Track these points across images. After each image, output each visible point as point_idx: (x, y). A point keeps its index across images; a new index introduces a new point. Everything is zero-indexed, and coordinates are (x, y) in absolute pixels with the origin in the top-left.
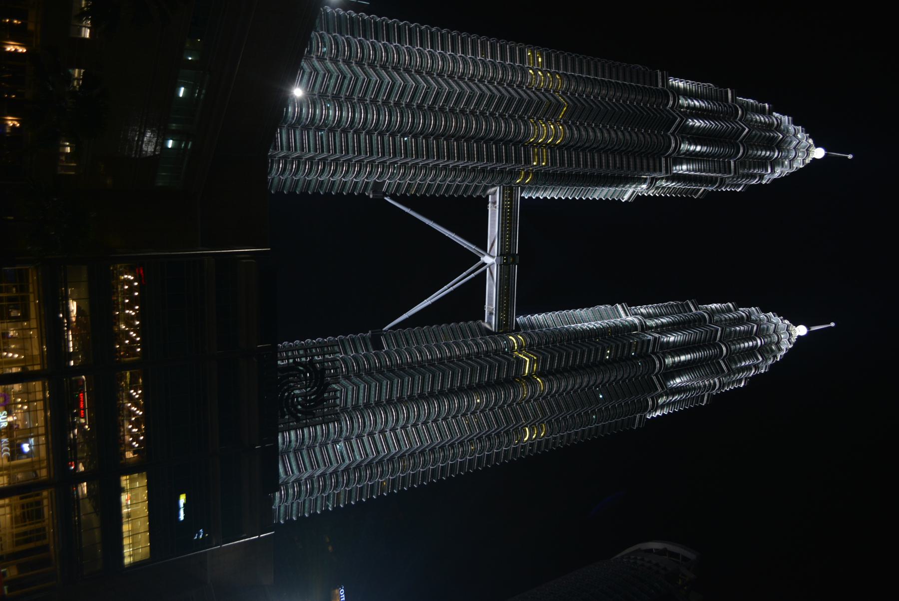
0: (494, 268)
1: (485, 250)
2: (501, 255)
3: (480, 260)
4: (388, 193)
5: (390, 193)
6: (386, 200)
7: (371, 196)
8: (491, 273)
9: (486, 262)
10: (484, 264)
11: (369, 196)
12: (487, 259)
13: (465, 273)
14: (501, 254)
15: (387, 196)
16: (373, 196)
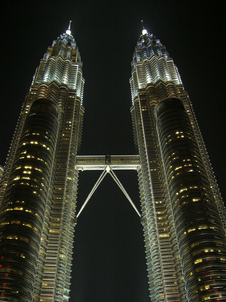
0: (112, 166)
1: (102, 171)
2: (106, 163)
3: (109, 173)
4: (75, 216)
5: (75, 215)
6: (78, 217)
7: (76, 224)
8: (115, 167)
9: (109, 170)
10: (110, 171)
11: (76, 225)
12: (108, 170)
13: (115, 179)
14: (106, 163)
15: (76, 217)
16: (76, 223)
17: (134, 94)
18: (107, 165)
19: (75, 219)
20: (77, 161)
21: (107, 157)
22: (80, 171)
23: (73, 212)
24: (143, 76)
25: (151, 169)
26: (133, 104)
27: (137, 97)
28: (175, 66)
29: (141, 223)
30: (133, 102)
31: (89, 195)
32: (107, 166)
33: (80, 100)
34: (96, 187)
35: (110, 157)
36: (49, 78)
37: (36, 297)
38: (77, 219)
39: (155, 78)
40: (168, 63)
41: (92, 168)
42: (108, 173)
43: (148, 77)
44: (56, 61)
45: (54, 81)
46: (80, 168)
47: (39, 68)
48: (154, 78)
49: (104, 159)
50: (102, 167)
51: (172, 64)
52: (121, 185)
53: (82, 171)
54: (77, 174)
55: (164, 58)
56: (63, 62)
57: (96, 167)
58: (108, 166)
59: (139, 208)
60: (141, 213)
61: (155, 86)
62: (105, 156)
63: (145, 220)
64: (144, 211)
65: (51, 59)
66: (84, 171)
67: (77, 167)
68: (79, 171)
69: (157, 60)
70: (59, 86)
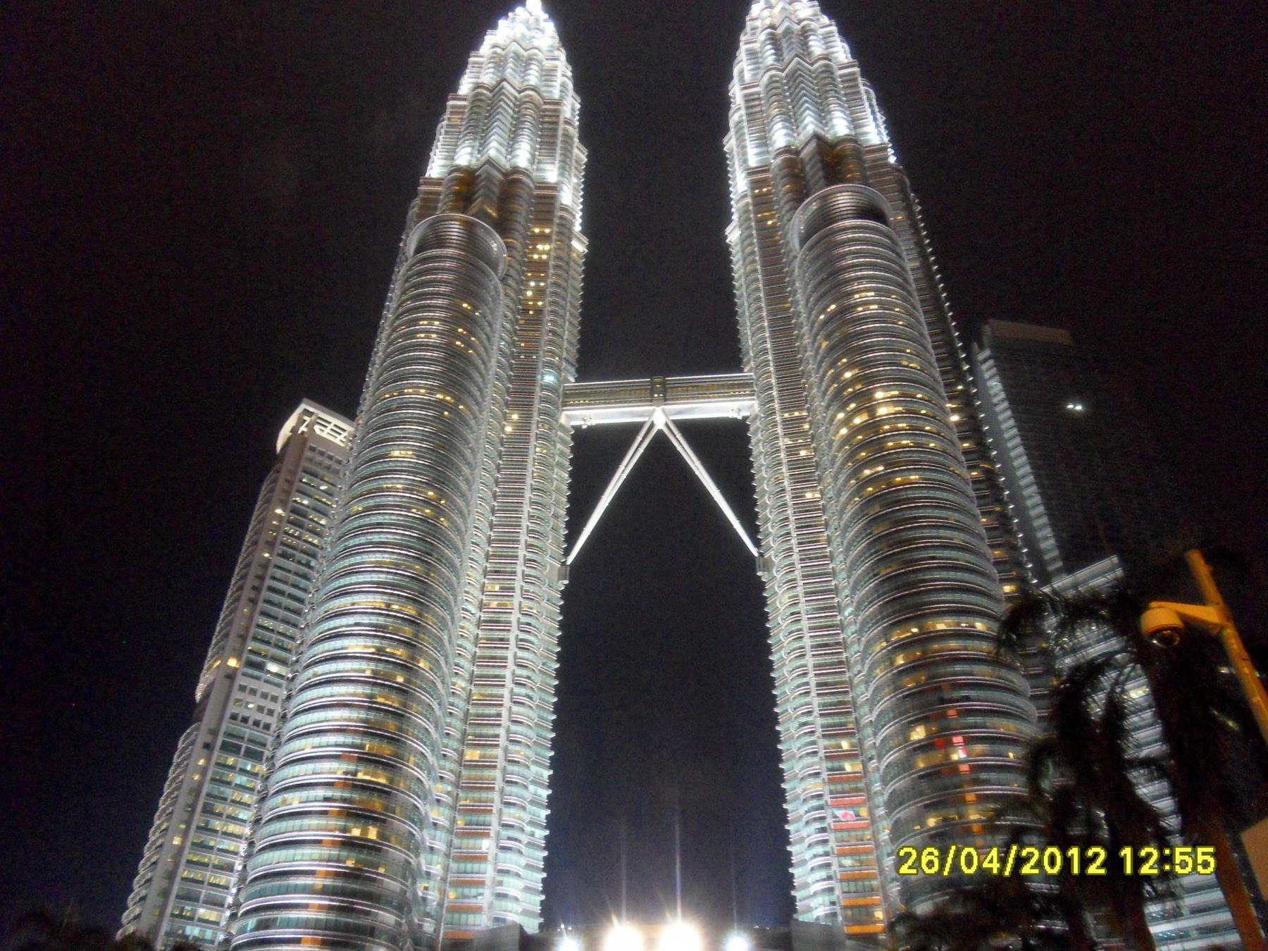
0: (669, 410)
1: (640, 425)
7: (566, 582)
8: (679, 413)
14: (651, 401)
15: (565, 562)
16: (565, 579)
17: (739, 184)
19: (564, 568)
20: (566, 400)
21: (653, 384)
22: (578, 429)
23: (559, 547)
24: (764, 124)
25: (784, 409)
26: (735, 217)
28: (864, 85)
29: (754, 571)
30: (733, 210)
32: (653, 411)
33: (574, 216)
34: (623, 473)
35: (664, 384)
36: (476, 152)
37: (449, 793)
38: (568, 568)
39: (800, 129)
40: (841, 76)
41: (612, 416)
42: (660, 433)
43: (776, 127)
44: (494, 96)
45: (490, 162)
46: (575, 418)
47: (445, 123)
48: (797, 127)
49: (646, 389)
50: (641, 415)
51: (856, 79)
53: (584, 427)
54: (569, 439)
55: (830, 60)
56: (516, 98)
57: (624, 414)
59: (753, 531)
60: (757, 543)
61: (797, 153)
63: (767, 566)
64: (765, 539)
65: (479, 90)
66: (590, 428)
67: (569, 417)
68: (573, 427)
69: (806, 71)
70: (506, 174)
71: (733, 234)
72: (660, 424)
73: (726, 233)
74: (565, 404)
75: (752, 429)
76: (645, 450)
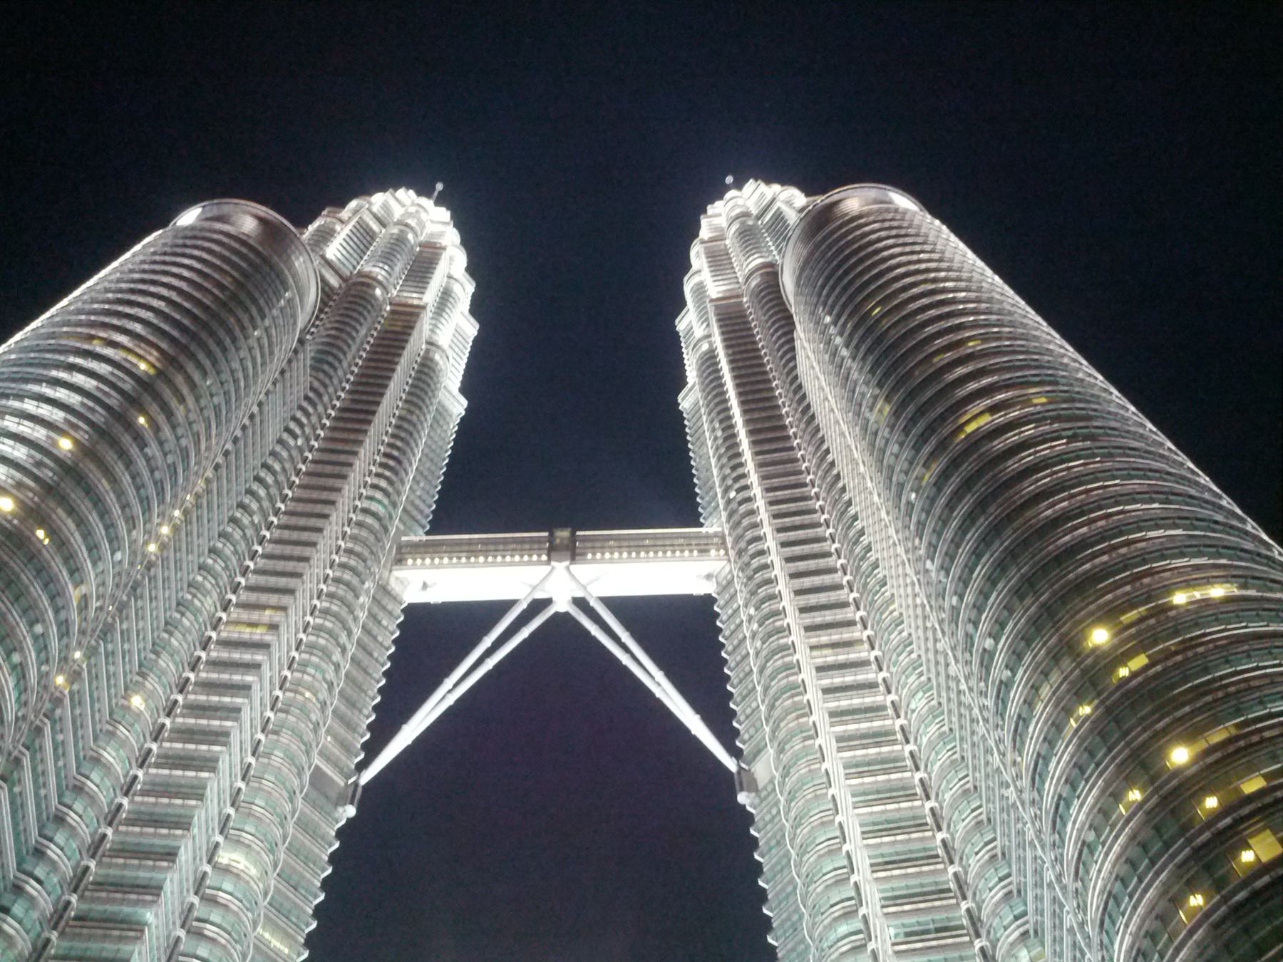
3: (567, 614)
7: (351, 811)
14: (548, 562)
16: (352, 803)
18: (553, 563)
21: (551, 539)
27: (709, 336)
31: (449, 683)
35: (573, 538)
38: (360, 790)
42: (562, 620)
52: (625, 637)
54: (398, 611)
58: (560, 566)
59: (727, 736)
60: (736, 753)
62: (546, 534)
71: (690, 400)
72: (562, 605)
73: (679, 401)
74: (399, 561)
75: (721, 602)
76: (533, 635)
